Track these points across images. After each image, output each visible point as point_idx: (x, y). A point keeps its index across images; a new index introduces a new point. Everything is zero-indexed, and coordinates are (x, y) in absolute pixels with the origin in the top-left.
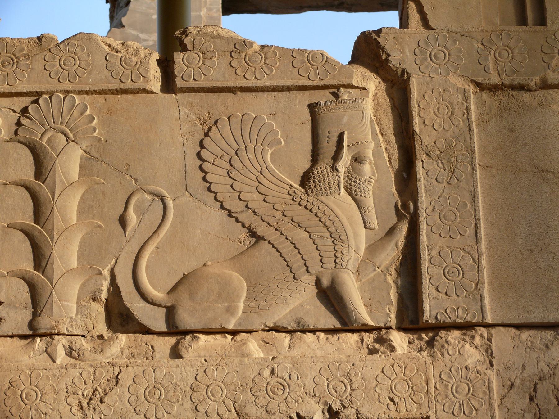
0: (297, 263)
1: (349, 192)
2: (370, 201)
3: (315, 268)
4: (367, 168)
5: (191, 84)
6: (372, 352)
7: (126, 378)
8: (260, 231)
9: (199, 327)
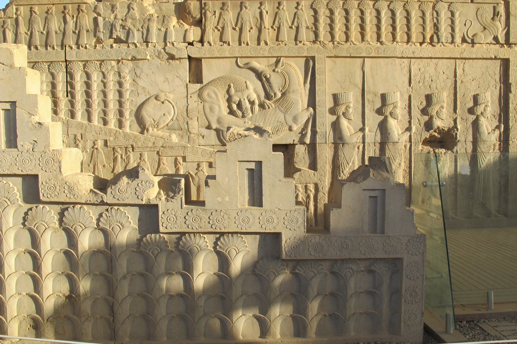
7: (466, 50)
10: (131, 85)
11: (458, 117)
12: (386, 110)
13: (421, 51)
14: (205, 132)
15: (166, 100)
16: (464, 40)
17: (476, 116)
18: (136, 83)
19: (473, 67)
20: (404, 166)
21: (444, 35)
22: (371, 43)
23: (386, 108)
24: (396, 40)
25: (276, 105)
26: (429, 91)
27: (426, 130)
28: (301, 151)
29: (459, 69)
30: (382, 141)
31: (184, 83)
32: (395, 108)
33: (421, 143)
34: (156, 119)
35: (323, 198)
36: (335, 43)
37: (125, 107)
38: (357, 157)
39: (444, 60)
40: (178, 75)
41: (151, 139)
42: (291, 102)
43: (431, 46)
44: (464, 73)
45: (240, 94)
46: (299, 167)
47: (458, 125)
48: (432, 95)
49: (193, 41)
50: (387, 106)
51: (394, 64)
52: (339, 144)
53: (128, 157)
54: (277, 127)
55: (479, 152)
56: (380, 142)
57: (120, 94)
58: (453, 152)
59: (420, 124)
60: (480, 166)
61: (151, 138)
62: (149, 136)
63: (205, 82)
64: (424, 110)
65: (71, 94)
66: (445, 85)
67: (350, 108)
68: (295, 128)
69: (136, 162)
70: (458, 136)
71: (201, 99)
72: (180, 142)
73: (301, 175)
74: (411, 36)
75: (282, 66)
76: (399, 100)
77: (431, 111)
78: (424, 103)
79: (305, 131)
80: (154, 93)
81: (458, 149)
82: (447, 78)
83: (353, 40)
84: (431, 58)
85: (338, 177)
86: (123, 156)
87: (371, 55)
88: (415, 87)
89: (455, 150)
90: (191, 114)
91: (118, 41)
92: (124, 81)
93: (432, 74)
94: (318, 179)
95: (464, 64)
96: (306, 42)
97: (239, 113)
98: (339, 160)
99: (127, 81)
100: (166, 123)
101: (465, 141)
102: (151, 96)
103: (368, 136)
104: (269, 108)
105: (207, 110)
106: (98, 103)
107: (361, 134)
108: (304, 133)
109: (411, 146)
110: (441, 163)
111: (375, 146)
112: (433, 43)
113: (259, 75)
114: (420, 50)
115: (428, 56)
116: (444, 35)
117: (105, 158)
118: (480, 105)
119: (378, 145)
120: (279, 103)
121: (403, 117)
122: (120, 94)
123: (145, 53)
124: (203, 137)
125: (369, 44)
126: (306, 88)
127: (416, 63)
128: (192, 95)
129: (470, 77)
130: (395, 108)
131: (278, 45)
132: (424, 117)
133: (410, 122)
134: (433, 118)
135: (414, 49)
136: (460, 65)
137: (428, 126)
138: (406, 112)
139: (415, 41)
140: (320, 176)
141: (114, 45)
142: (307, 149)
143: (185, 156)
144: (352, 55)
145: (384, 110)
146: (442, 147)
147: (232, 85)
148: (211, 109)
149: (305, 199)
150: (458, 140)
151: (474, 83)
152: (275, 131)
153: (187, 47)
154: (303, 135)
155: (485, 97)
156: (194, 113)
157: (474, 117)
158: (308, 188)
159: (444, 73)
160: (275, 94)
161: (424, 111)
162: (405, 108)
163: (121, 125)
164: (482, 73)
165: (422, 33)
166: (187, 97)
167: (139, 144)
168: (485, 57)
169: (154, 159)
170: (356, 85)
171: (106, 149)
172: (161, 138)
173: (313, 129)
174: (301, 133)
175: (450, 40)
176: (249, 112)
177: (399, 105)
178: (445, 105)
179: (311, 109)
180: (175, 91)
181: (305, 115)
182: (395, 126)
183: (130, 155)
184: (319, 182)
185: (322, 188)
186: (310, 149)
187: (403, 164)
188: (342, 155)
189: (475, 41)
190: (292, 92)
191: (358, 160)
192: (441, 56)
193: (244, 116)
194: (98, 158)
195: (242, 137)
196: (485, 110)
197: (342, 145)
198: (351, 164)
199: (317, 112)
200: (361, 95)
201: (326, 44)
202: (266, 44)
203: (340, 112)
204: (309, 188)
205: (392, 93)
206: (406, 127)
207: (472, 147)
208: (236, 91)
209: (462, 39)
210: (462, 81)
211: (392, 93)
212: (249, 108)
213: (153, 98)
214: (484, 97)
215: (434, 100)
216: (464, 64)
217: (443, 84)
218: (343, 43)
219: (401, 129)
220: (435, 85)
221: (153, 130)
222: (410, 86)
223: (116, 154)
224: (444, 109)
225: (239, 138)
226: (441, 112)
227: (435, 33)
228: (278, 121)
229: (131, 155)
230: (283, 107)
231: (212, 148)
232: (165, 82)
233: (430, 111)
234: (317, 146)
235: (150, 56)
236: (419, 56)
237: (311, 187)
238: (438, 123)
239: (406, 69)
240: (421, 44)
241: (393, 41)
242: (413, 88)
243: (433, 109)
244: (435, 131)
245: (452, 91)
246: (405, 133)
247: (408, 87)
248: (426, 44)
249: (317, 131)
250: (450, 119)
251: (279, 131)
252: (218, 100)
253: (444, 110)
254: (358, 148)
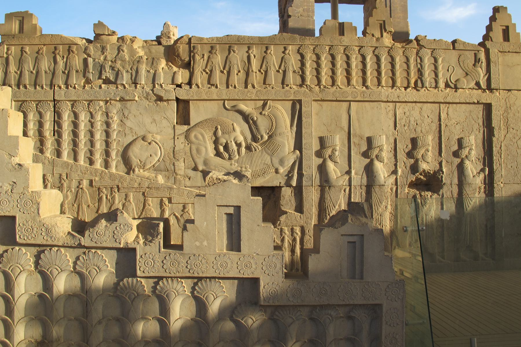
0: (474, 79)
1: (481, 67)
2: (483, 69)
3: (476, 79)
4: (483, 64)
5: (458, 49)
6: (483, 92)
7: (450, 95)
8: (468, 73)
9: (460, 87)
10: (118, 125)
11: (443, 160)
12: (372, 153)
13: (406, 95)
14: (191, 173)
15: (153, 141)
16: (447, 85)
17: (460, 159)
18: (124, 123)
19: (456, 111)
20: (390, 209)
21: (428, 80)
22: (357, 87)
23: (372, 151)
24: (381, 85)
25: (263, 148)
26: (414, 134)
27: (411, 173)
28: (287, 193)
29: (443, 113)
30: (368, 184)
31: (171, 124)
32: (381, 151)
33: (407, 186)
34: (143, 160)
35: (310, 241)
36: (322, 87)
37: (112, 148)
38: (344, 200)
39: (429, 104)
40: (165, 116)
41: (137, 179)
42: (277, 145)
43: (415, 91)
44: (448, 116)
45: (227, 136)
46: (285, 210)
47: (443, 168)
48: (417, 138)
49: (181, 83)
50: (373, 149)
51: (379, 108)
52: (325, 186)
53: (113, 198)
54: (263, 169)
55: (464, 194)
56: (366, 185)
57: (108, 134)
58: (439, 195)
59: (406, 167)
60: (466, 209)
61: (137, 178)
62: (135, 177)
63: (192, 123)
64: (410, 153)
65: (58, 133)
66: (430, 128)
67: (336, 151)
68: (281, 170)
69: (121, 203)
70: (443, 179)
71: (188, 141)
72: (166, 184)
73: (287, 217)
74: (396, 81)
75: (269, 109)
76: (384, 144)
77: (417, 154)
78: (410, 146)
79: (292, 174)
80: (141, 133)
81: (444, 192)
82: (432, 122)
83: (339, 84)
84: (415, 102)
85: (324, 220)
86: (108, 197)
87: (357, 99)
88: (400, 131)
89: (441, 193)
90: (178, 155)
91: (107, 81)
92: (111, 122)
93: (417, 118)
94: (304, 222)
95: (448, 108)
96: (293, 86)
97: (226, 155)
98: (325, 203)
99: (115, 121)
100: (153, 164)
101: (451, 184)
102: (138, 136)
103: (354, 179)
104: (255, 150)
105: (194, 152)
106: (85, 143)
107: (347, 177)
108: (290, 175)
109: (397, 189)
110: (428, 206)
111: (361, 189)
112: (417, 88)
113: (246, 118)
114: (405, 94)
115: (412, 101)
116: (428, 80)
117: (90, 198)
118: (464, 148)
119: (364, 188)
120: (265, 145)
121: (388, 160)
122: (108, 134)
123: (134, 94)
124: (189, 179)
125: (355, 88)
126: (292, 131)
127: (401, 107)
128: (179, 137)
129: (454, 121)
130: (381, 151)
131: (265, 88)
132: (410, 160)
133: (396, 165)
134: (418, 162)
135: (399, 93)
136: (444, 109)
137: (414, 168)
138: (392, 155)
139: (399, 86)
140: (307, 218)
141: (103, 86)
142: (293, 192)
143: (171, 198)
144: (338, 99)
145: (370, 153)
146: (427, 191)
147: (219, 127)
148: (198, 151)
149: (291, 242)
150: (444, 182)
151: (458, 127)
152: (261, 173)
153: (175, 89)
154: (289, 177)
155: (470, 141)
156: (181, 154)
157: (459, 160)
158: (294, 231)
159: (428, 117)
160: (262, 137)
161: (410, 155)
162: (391, 151)
163: (107, 165)
164: (466, 117)
165: (406, 78)
166: (174, 138)
167: (125, 184)
168: (468, 101)
169: (139, 200)
170: (342, 129)
171: (91, 189)
172: (147, 178)
173: (300, 172)
174: (287, 175)
175: (434, 85)
176: (235, 154)
177: (385, 148)
178: (430, 148)
179: (298, 152)
180: (162, 132)
181: (291, 157)
182: (381, 169)
183: (115, 195)
184: (305, 225)
185: (308, 231)
186: (297, 191)
187: (389, 207)
188: (329, 198)
189: (458, 86)
190: (279, 134)
191: (345, 204)
192: (425, 101)
193: (231, 158)
194: (83, 198)
195: (221, 181)
196: (469, 153)
197: (329, 188)
198: (337, 207)
199: (303, 154)
200: (347, 138)
201: (312, 88)
202: (254, 87)
203: (326, 154)
204: (295, 231)
205: (378, 136)
206: (392, 170)
207: (457, 190)
208: (223, 133)
209: (445, 84)
210: (446, 125)
211: (378, 136)
212: (236, 150)
213: (140, 138)
214: (468, 141)
215: (420, 143)
216: (448, 108)
217: (428, 128)
218: (329, 87)
219: (387, 172)
220: (420, 129)
221: (139, 171)
222: (395, 129)
223: (102, 194)
224: (430, 152)
225: (218, 183)
226: (427, 155)
227: (419, 77)
228: (264, 164)
229: (117, 196)
230: (269, 150)
231: (197, 189)
232: (153, 123)
233: (415, 154)
234: (304, 189)
235: (138, 98)
236: (403, 100)
237: (298, 230)
238: (423, 166)
239: (391, 113)
240: (406, 89)
241: (378, 85)
242: (398, 131)
243: (418, 152)
244: (421, 174)
245: (437, 135)
246: (391, 176)
247: (394, 131)
248: (411, 88)
249: (303, 174)
250: (435, 162)
251: (265, 174)
252: (205, 142)
253: (430, 154)
254: (345, 191)
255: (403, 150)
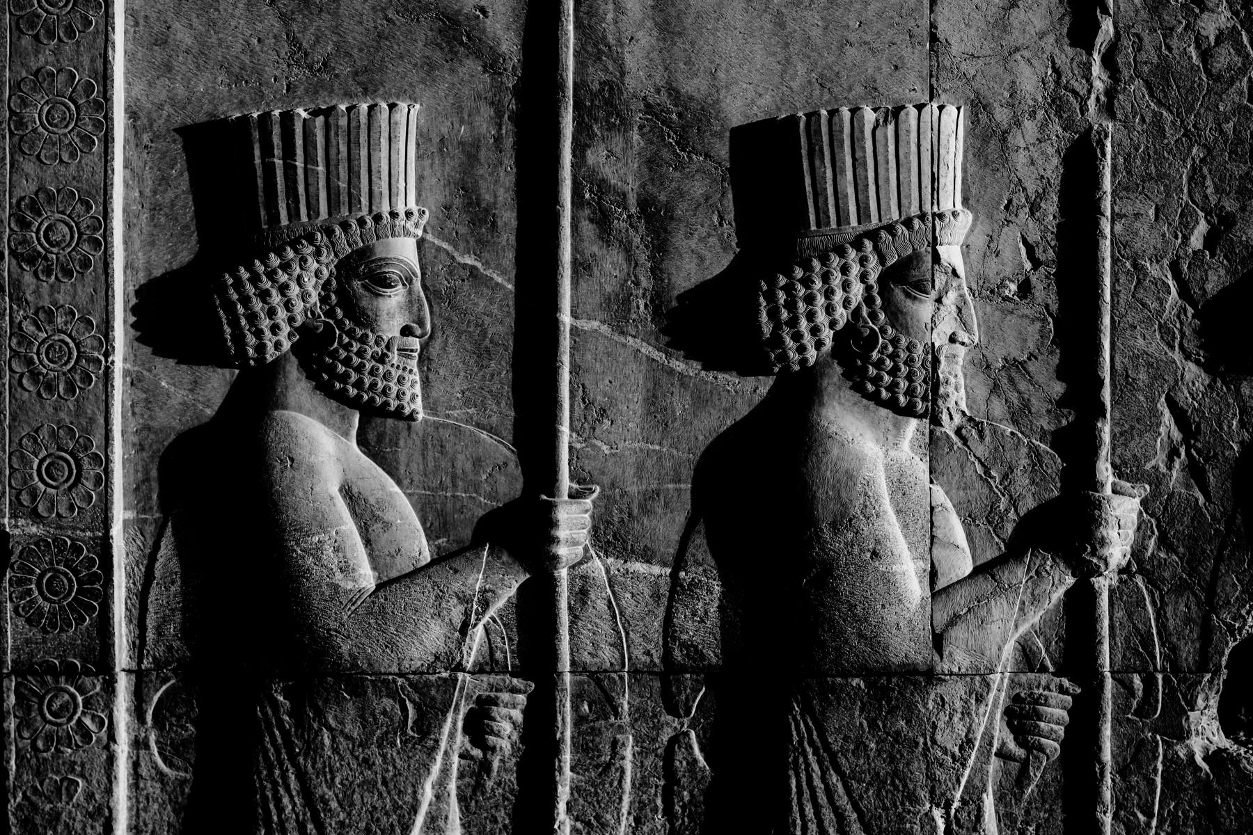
12: (791, 305)
23: (789, 289)
50: (808, 267)
76: (950, 198)
121: (995, 389)
145: (773, 314)
162: (1025, 289)
177: (951, 254)
255: (1175, 268)
